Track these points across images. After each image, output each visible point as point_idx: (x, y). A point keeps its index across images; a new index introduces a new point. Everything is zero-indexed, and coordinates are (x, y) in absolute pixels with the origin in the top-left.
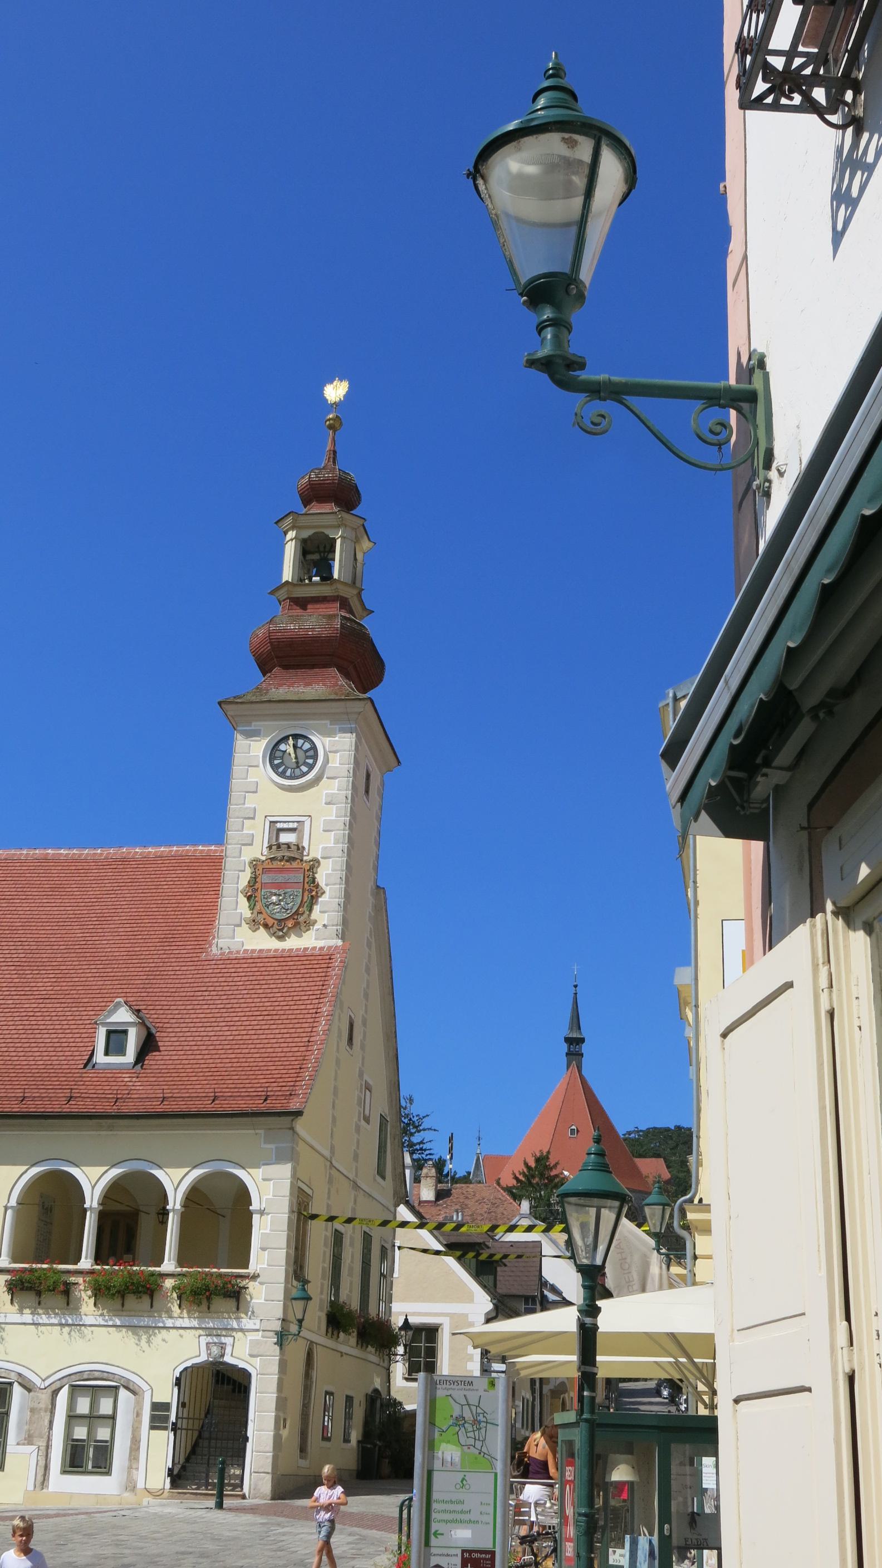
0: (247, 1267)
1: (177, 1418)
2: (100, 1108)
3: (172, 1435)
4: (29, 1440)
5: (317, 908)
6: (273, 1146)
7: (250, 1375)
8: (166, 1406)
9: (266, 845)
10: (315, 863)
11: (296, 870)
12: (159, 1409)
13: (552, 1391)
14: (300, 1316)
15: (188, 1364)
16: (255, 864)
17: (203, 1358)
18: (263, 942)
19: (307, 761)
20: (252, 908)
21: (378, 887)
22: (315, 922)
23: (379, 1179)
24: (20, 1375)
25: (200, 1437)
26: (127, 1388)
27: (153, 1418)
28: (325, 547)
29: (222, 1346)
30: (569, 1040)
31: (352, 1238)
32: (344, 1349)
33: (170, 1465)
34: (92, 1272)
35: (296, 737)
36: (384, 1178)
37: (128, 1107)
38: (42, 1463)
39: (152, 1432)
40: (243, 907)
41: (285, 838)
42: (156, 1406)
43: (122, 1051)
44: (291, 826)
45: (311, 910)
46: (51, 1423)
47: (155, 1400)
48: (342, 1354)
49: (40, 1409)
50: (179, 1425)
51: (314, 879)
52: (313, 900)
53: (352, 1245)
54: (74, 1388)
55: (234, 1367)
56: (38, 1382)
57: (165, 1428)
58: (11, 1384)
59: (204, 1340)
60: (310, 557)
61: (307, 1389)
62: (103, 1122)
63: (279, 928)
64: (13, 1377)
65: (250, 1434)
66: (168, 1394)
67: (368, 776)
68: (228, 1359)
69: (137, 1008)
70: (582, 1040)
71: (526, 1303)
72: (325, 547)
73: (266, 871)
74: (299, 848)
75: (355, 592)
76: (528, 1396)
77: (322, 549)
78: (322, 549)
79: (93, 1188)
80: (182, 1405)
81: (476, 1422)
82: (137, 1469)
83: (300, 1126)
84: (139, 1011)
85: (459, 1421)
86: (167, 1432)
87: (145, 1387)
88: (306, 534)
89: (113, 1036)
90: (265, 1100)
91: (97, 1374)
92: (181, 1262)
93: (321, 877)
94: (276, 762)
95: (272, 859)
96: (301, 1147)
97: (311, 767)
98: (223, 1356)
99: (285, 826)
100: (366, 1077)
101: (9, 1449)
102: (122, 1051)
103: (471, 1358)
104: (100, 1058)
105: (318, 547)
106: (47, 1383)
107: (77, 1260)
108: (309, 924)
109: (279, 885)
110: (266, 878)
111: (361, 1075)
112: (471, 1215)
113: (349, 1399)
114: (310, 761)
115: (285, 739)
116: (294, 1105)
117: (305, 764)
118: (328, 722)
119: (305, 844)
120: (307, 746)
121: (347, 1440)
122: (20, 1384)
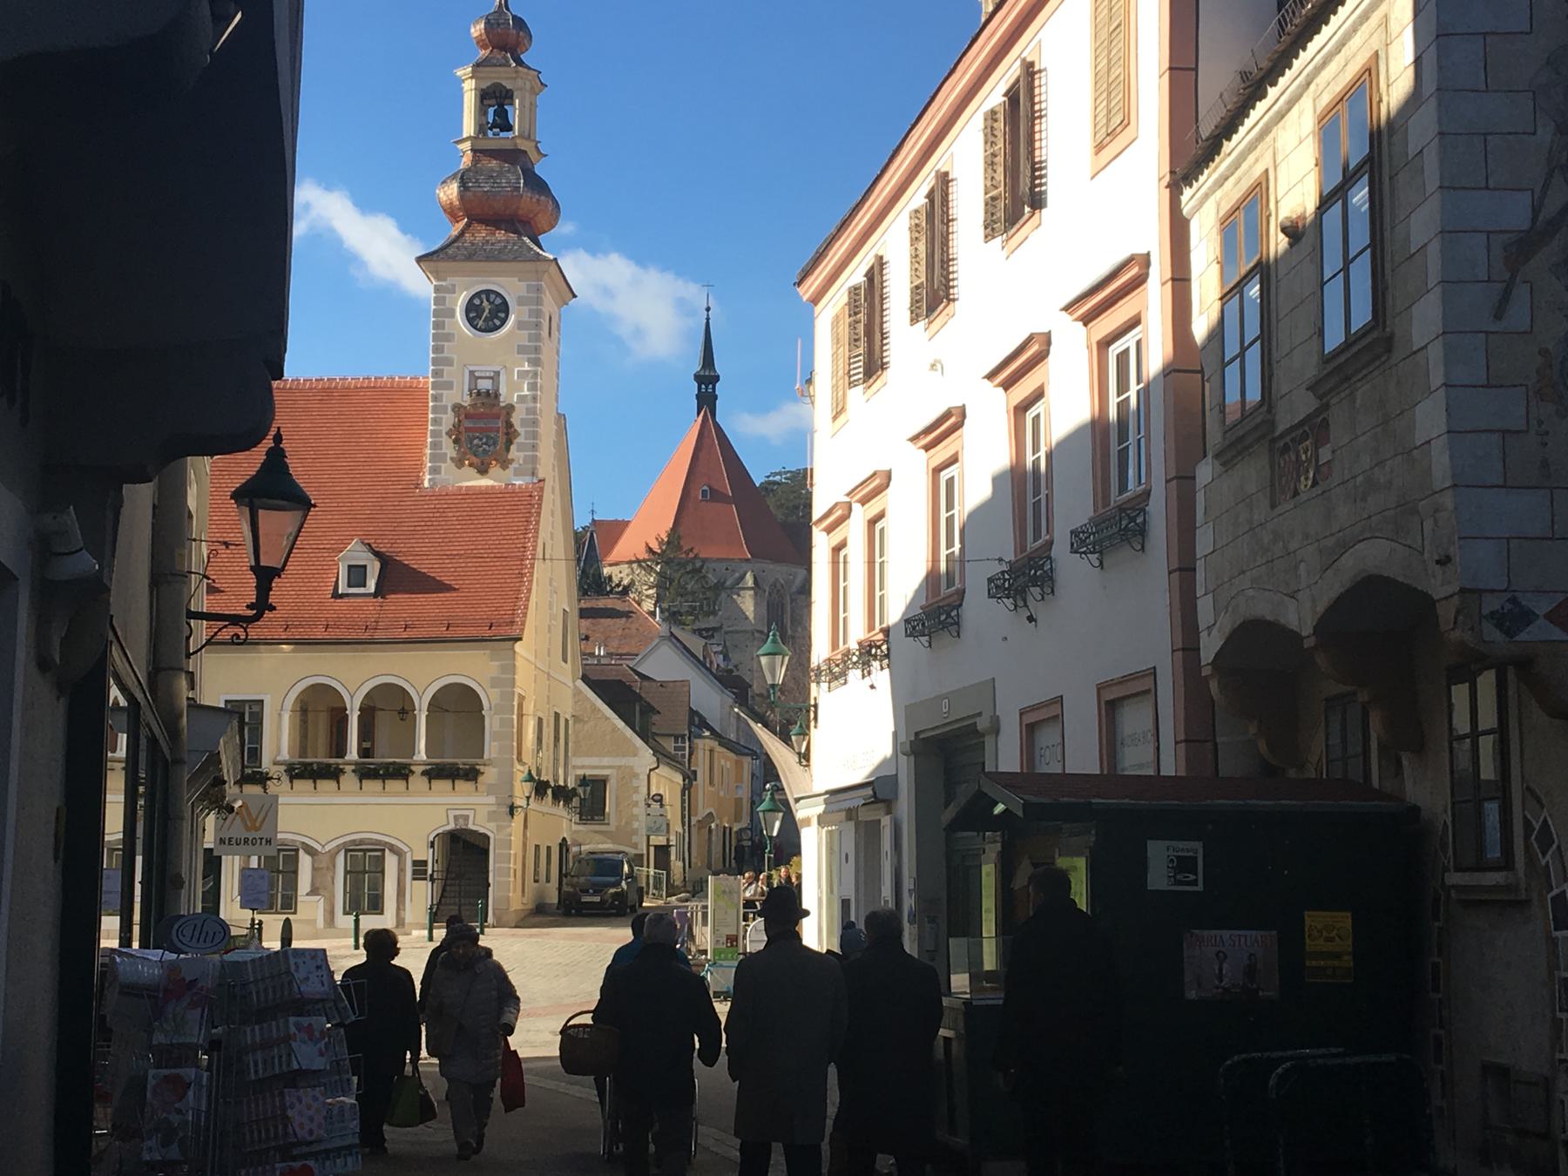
0: (482, 757)
2: (353, 635)
3: (430, 884)
4: (314, 891)
5: (513, 448)
6: (497, 663)
7: (488, 838)
8: (425, 863)
9: (466, 391)
10: (510, 408)
11: (497, 417)
12: (420, 866)
13: (699, 821)
14: (527, 795)
15: (440, 831)
16: (457, 408)
17: (451, 826)
19: (500, 314)
21: (558, 414)
22: (513, 460)
23: (563, 664)
25: (445, 885)
26: (390, 850)
27: (415, 872)
28: (501, 92)
29: (466, 818)
30: (697, 377)
31: (548, 721)
32: (545, 809)
34: (356, 764)
35: (488, 292)
36: (566, 662)
37: (379, 635)
38: (328, 908)
39: (414, 882)
40: (449, 449)
41: (485, 385)
42: (415, 863)
44: (488, 374)
45: (508, 450)
46: (333, 878)
47: (415, 859)
48: (544, 814)
49: (322, 869)
50: (435, 876)
51: (509, 425)
52: (509, 442)
53: (548, 726)
54: (347, 851)
55: (475, 832)
56: (319, 848)
57: (425, 879)
58: (297, 851)
59: (452, 814)
60: (486, 102)
61: (525, 845)
62: (357, 646)
64: (298, 844)
65: (491, 881)
66: (425, 854)
67: (550, 318)
68: (471, 826)
69: (366, 541)
70: (717, 378)
71: (676, 742)
72: (501, 92)
73: (467, 417)
74: (497, 395)
75: (534, 144)
76: (681, 830)
77: (498, 94)
78: (498, 94)
79: (352, 697)
80: (435, 861)
81: (730, 892)
82: (404, 910)
83: (518, 646)
84: (369, 545)
85: (724, 892)
87: (406, 849)
88: (485, 85)
89: (353, 569)
90: (491, 627)
91: (367, 841)
92: (428, 757)
93: (516, 419)
94: (471, 315)
95: (473, 406)
96: (519, 663)
97: (504, 321)
98: (467, 825)
99: (483, 375)
100: (554, 584)
101: (299, 899)
103: (636, 804)
105: (494, 92)
106: (327, 848)
107: (343, 757)
109: (481, 430)
110: (468, 424)
111: (551, 585)
112: (602, 633)
113: (549, 848)
114: (502, 315)
115: (478, 295)
116: (515, 633)
117: (498, 318)
118: (516, 279)
119: (503, 390)
120: (498, 301)
121: (548, 881)
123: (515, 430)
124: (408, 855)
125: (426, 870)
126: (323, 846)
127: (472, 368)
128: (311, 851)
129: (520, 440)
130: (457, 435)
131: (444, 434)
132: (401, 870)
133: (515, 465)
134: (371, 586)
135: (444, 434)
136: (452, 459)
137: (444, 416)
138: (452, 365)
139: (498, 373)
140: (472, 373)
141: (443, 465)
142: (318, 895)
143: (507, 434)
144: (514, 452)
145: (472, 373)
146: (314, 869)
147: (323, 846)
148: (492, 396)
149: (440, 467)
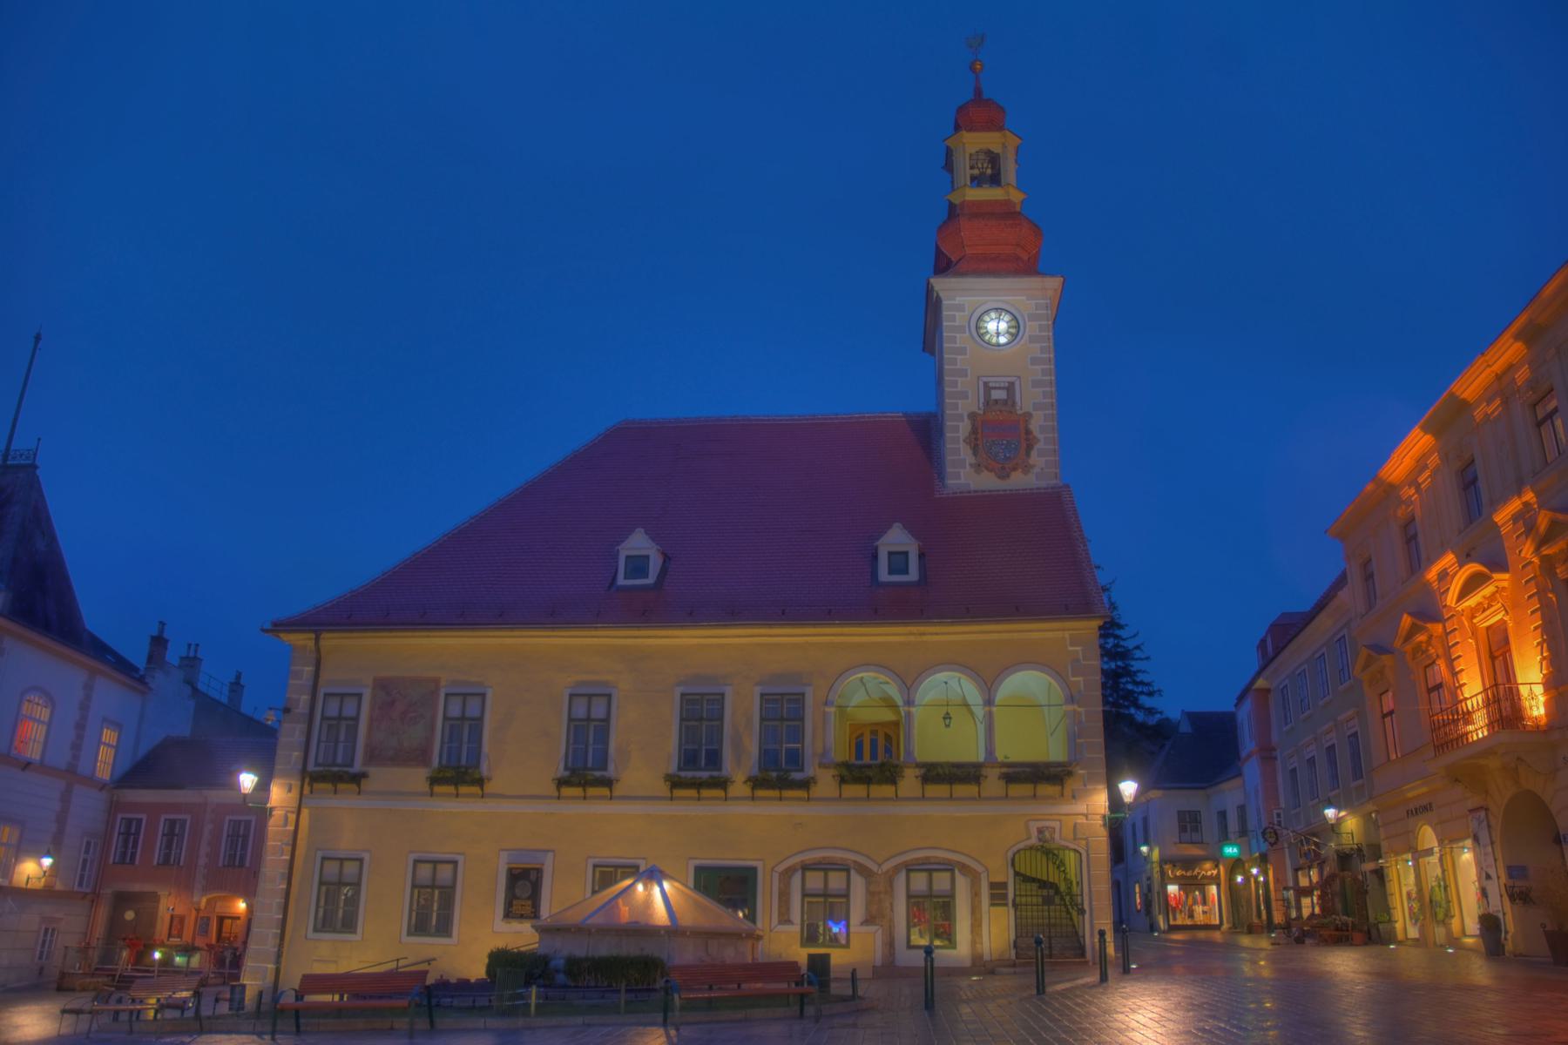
1: (1015, 895)
3: (1012, 911)
4: (869, 920)
5: (1034, 453)
8: (1004, 885)
9: (982, 400)
10: (1028, 415)
16: (972, 416)
18: (987, 482)
20: (975, 453)
24: (855, 862)
27: (993, 897)
33: (1013, 937)
39: (992, 908)
40: (966, 453)
42: (993, 886)
43: (905, 571)
44: (1002, 385)
45: (1028, 454)
47: (993, 880)
51: (1028, 432)
52: (1029, 448)
54: (909, 871)
56: (874, 868)
57: (1006, 905)
63: (1004, 474)
86: (1005, 908)
87: (979, 868)
91: (932, 861)
93: (1035, 425)
99: (997, 385)
102: (905, 571)
104: (884, 575)
106: (886, 867)
108: (1027, 469)
122: (856, 870)
123: (1035, 437)
124: (984, 876)
125: (1005, 896)
126: (880, 865)
127: (985, 379)
128: (864, 871)
129: (1039, 446)
130: (974, 441)
131: (961, 441)
132: (975, 894)
133: (1036, 470)
134: (913, 575)
135: (961, 441)
136: (971, 465)
137: (961, 424)
138: (966, 376)
139: (1012, 384)
140: (986, 384)
141: (962, 471)
142: (876, 925)
143: (1027, 440)
144: (1036, 459)
145: (986, 384)
146: (870, 894)
147: (880, 865)
148: (1010, 401)
149: (959, 473)
